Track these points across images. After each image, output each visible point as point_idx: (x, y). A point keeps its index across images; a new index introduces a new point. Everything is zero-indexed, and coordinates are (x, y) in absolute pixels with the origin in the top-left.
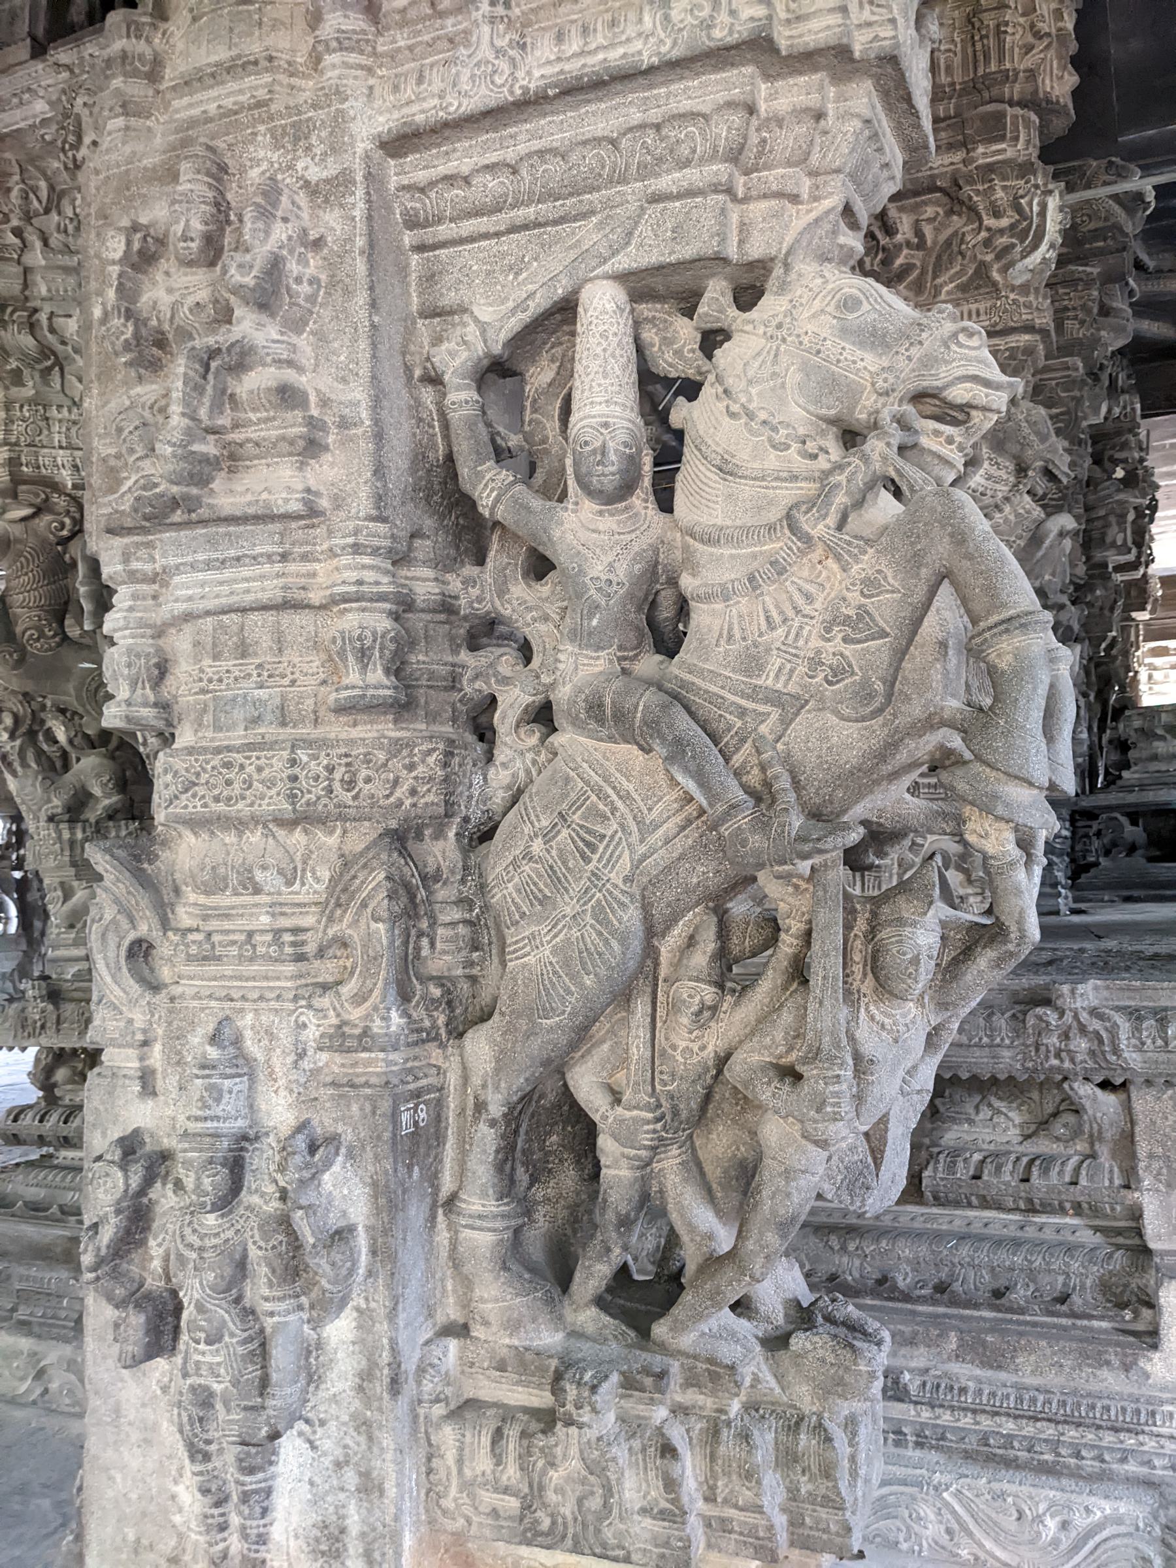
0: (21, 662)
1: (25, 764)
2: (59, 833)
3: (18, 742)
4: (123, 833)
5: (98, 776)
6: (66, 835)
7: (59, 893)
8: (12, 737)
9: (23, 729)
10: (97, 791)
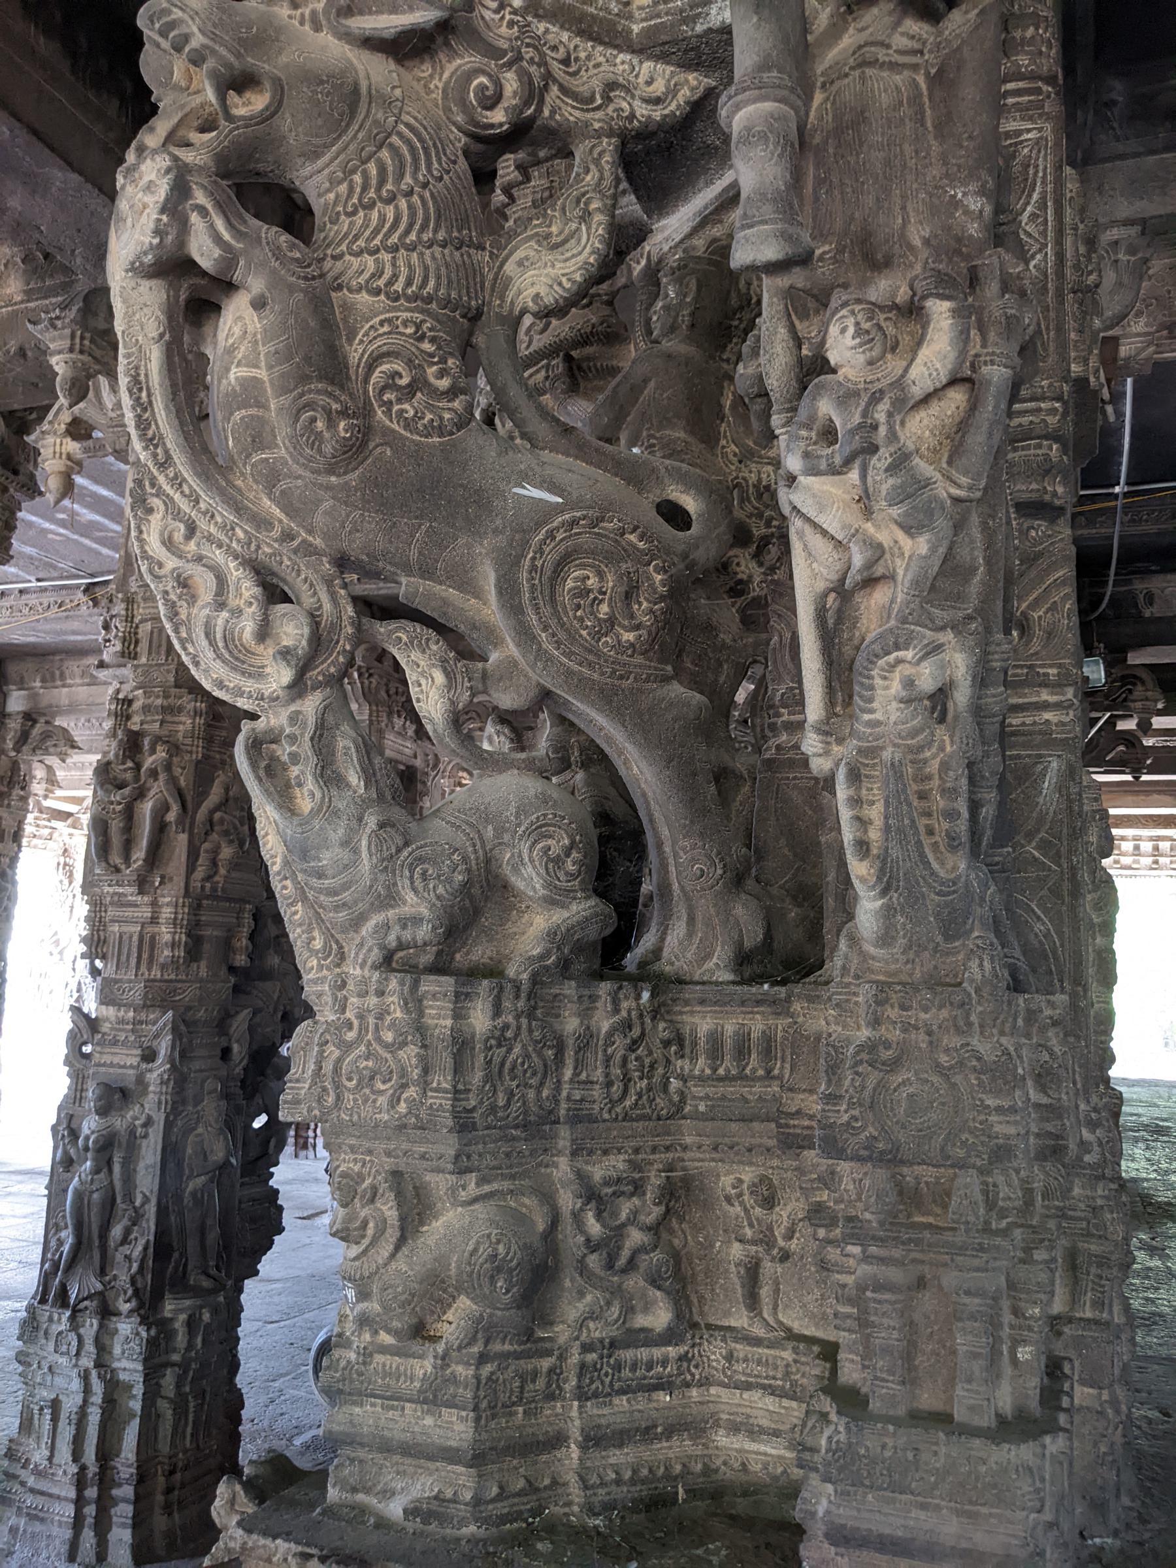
0: (355, 449)
1: (328, 776)
2: (415, 1003)
3: (311, 705)
4: (604, 1024)
5: (539, 832)
6: (439, 1018)
7: (389, 1210)
8: (298, 688)
9: (328, 665)
10: (529, 879)
